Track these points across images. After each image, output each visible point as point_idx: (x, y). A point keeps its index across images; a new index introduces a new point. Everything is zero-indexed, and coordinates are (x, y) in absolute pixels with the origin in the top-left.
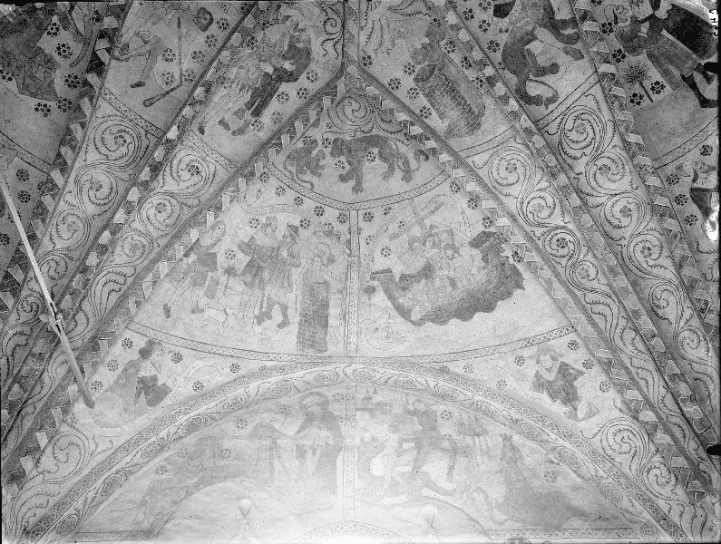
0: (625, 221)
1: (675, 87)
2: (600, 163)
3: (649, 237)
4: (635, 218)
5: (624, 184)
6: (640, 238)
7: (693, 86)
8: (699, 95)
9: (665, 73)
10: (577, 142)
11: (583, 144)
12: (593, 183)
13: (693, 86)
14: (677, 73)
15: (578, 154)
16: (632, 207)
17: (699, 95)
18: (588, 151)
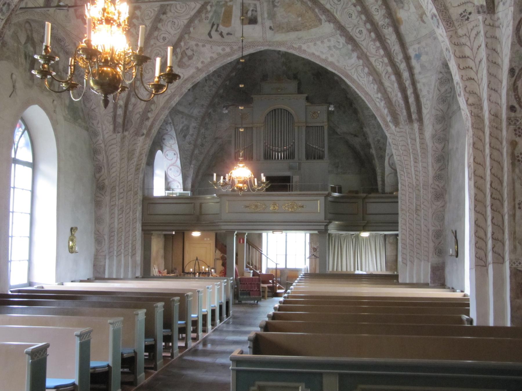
0: (161, 41)
1: (210, 23)
2: (175, 20)
3: (162, 52)
4: (163, 44)
5: (173, 32)
6: (160, 49)
7: (212, 27)
8: (210, 31)
9: (212, 17)
10: (176, 8)
11: (177, 11)
12: (166, 23)
13: (212, 27)
14: (214, 20)
15: (173, 11)
16: (167, 39)
17: (210, 31)
18: (176, 14)
